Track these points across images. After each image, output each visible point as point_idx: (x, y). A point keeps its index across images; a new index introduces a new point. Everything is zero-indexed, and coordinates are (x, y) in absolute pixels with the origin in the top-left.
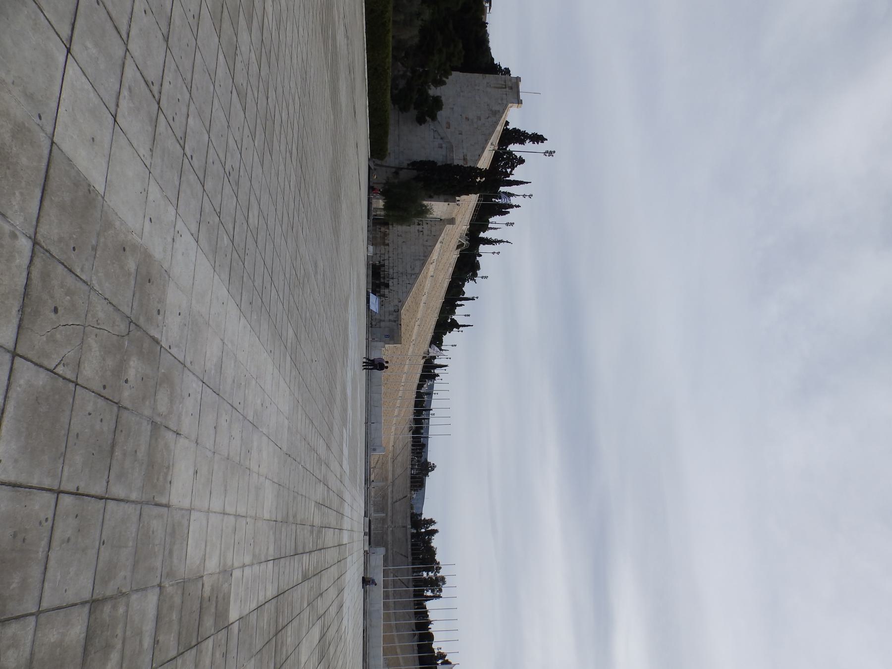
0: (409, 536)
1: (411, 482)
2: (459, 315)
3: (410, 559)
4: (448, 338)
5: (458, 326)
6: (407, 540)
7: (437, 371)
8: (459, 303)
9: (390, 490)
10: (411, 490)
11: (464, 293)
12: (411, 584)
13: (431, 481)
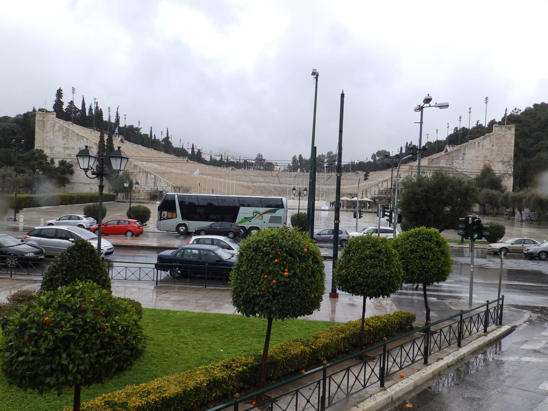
1: (268, 170)
2: (160, 137)
4: (175, 144)
5: (167, 138)
7: (196, 151)
8: (153, 138)
9: (272, 185)
10: (273, 170)
11: (147, 135)
13: (268, 157)
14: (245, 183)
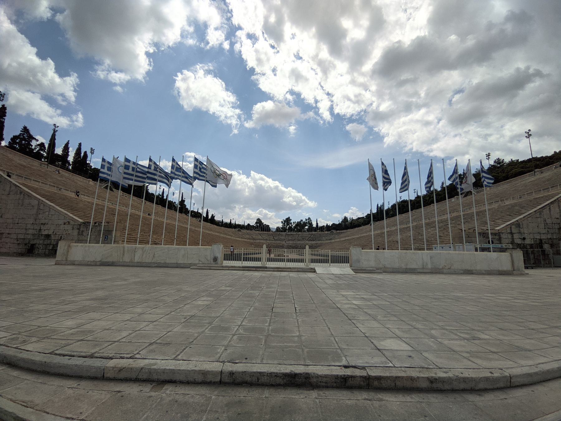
0: (290, 233)
3: (300, 233)
6: (292, 234)
10: (269, 231)
12: (311, 233)
14: (249, 240)
